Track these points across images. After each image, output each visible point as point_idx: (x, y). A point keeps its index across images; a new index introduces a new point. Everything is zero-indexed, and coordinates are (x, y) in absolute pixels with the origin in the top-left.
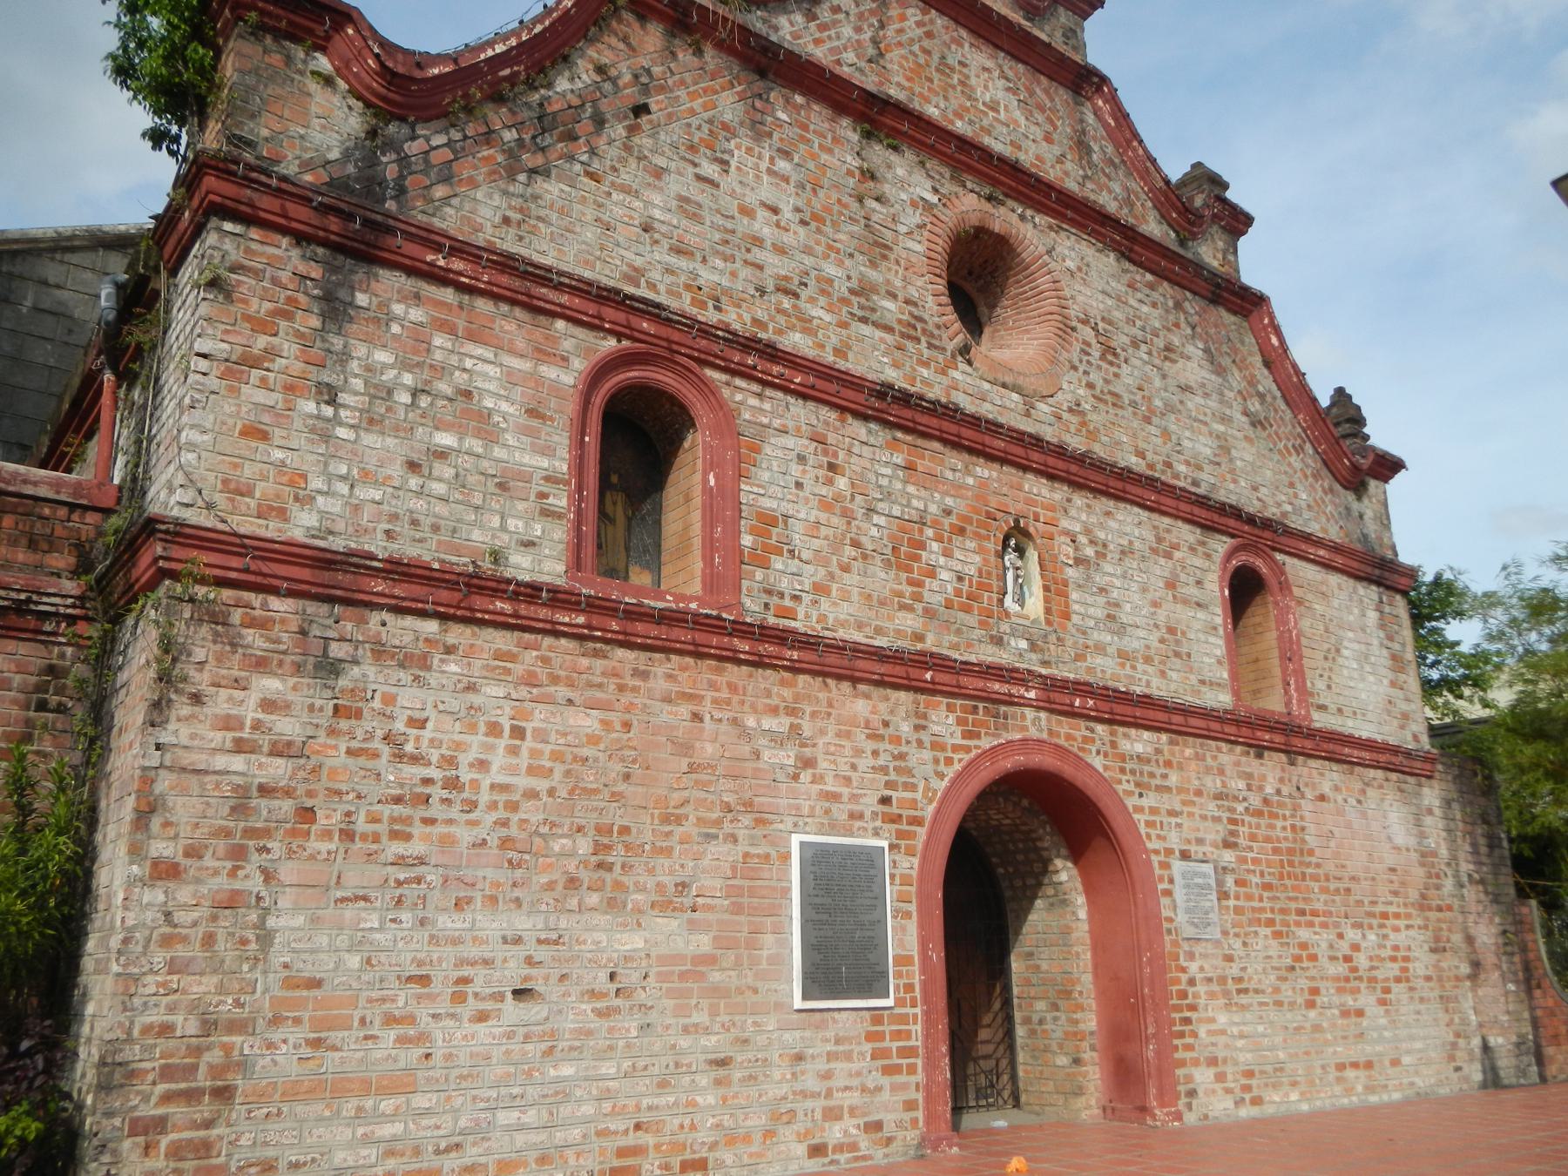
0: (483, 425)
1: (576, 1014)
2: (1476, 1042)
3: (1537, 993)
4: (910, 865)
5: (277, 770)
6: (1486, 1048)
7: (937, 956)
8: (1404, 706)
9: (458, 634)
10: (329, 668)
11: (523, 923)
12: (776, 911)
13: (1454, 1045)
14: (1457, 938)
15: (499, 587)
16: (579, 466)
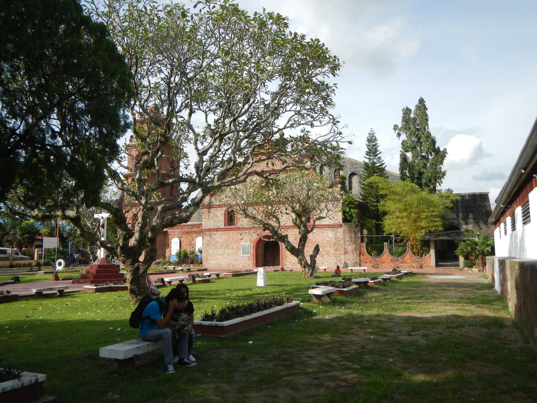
0: (218, 217)
1: (226, 256)
2: (343, 262)
3: (362, 256)
4: (252, 245)
5: (208, 242)
6: (345, 263)
7: (255, 252)
8: (337, 218)
9: (218, 232)
10: (210, 236)
11: (222, 250)
12: (240, 249)
13: (337, 262)
14: (342, 249)
15: (219, 229)
16: (225, 218)
